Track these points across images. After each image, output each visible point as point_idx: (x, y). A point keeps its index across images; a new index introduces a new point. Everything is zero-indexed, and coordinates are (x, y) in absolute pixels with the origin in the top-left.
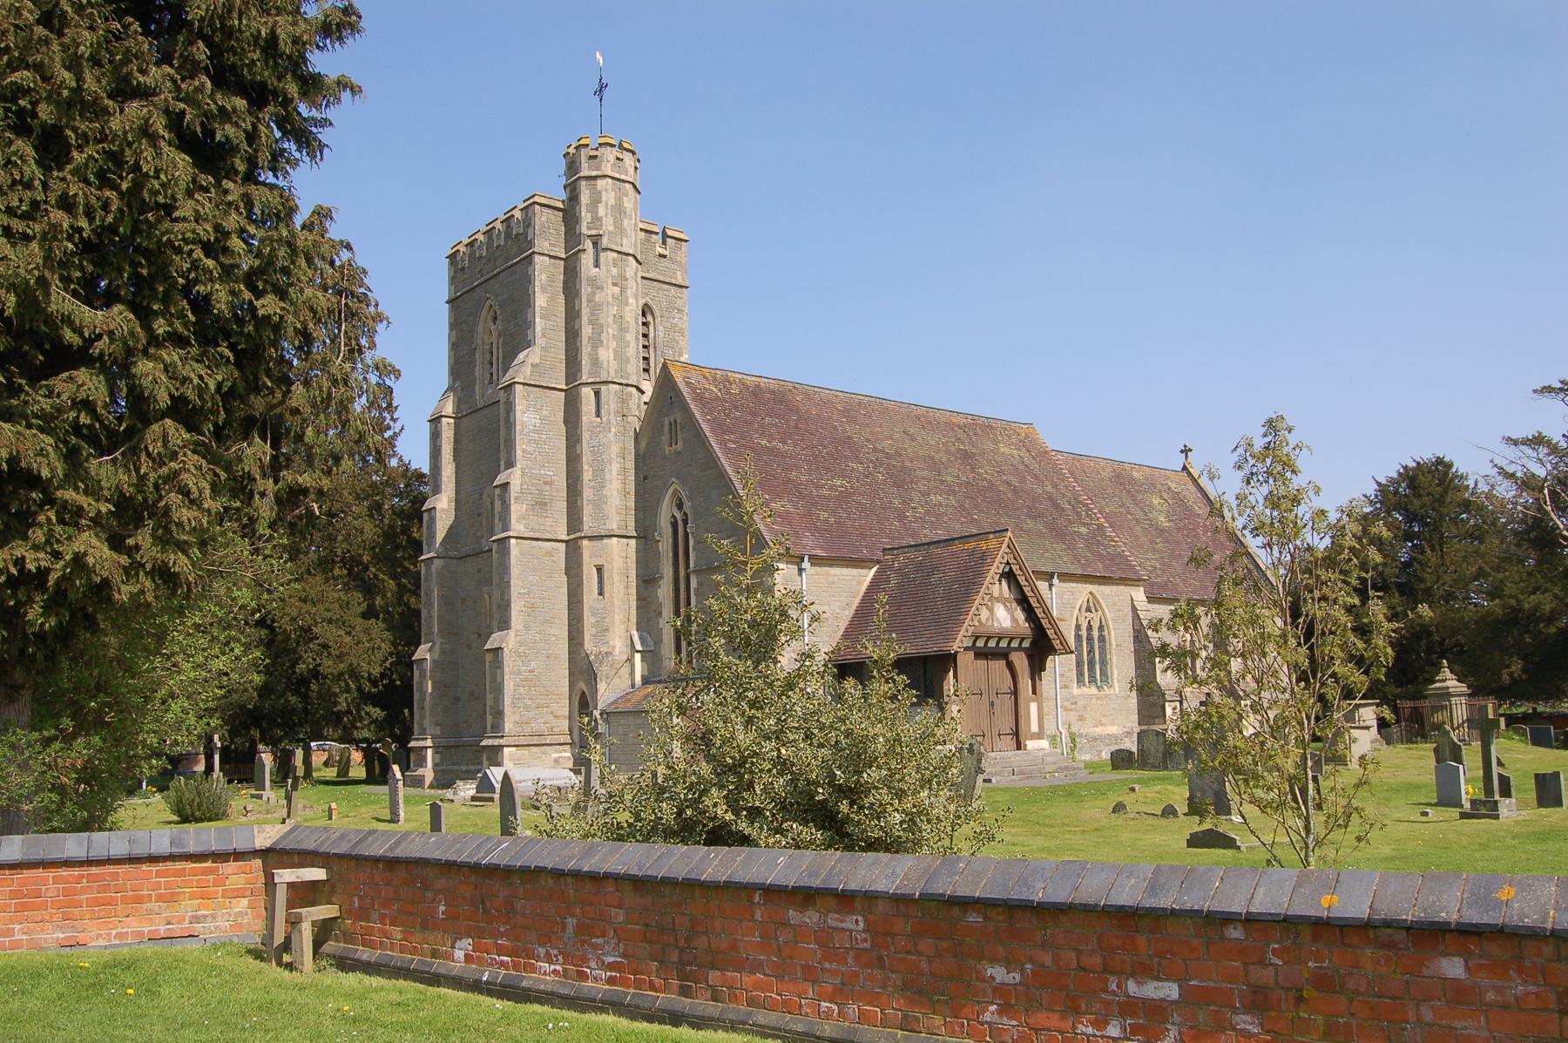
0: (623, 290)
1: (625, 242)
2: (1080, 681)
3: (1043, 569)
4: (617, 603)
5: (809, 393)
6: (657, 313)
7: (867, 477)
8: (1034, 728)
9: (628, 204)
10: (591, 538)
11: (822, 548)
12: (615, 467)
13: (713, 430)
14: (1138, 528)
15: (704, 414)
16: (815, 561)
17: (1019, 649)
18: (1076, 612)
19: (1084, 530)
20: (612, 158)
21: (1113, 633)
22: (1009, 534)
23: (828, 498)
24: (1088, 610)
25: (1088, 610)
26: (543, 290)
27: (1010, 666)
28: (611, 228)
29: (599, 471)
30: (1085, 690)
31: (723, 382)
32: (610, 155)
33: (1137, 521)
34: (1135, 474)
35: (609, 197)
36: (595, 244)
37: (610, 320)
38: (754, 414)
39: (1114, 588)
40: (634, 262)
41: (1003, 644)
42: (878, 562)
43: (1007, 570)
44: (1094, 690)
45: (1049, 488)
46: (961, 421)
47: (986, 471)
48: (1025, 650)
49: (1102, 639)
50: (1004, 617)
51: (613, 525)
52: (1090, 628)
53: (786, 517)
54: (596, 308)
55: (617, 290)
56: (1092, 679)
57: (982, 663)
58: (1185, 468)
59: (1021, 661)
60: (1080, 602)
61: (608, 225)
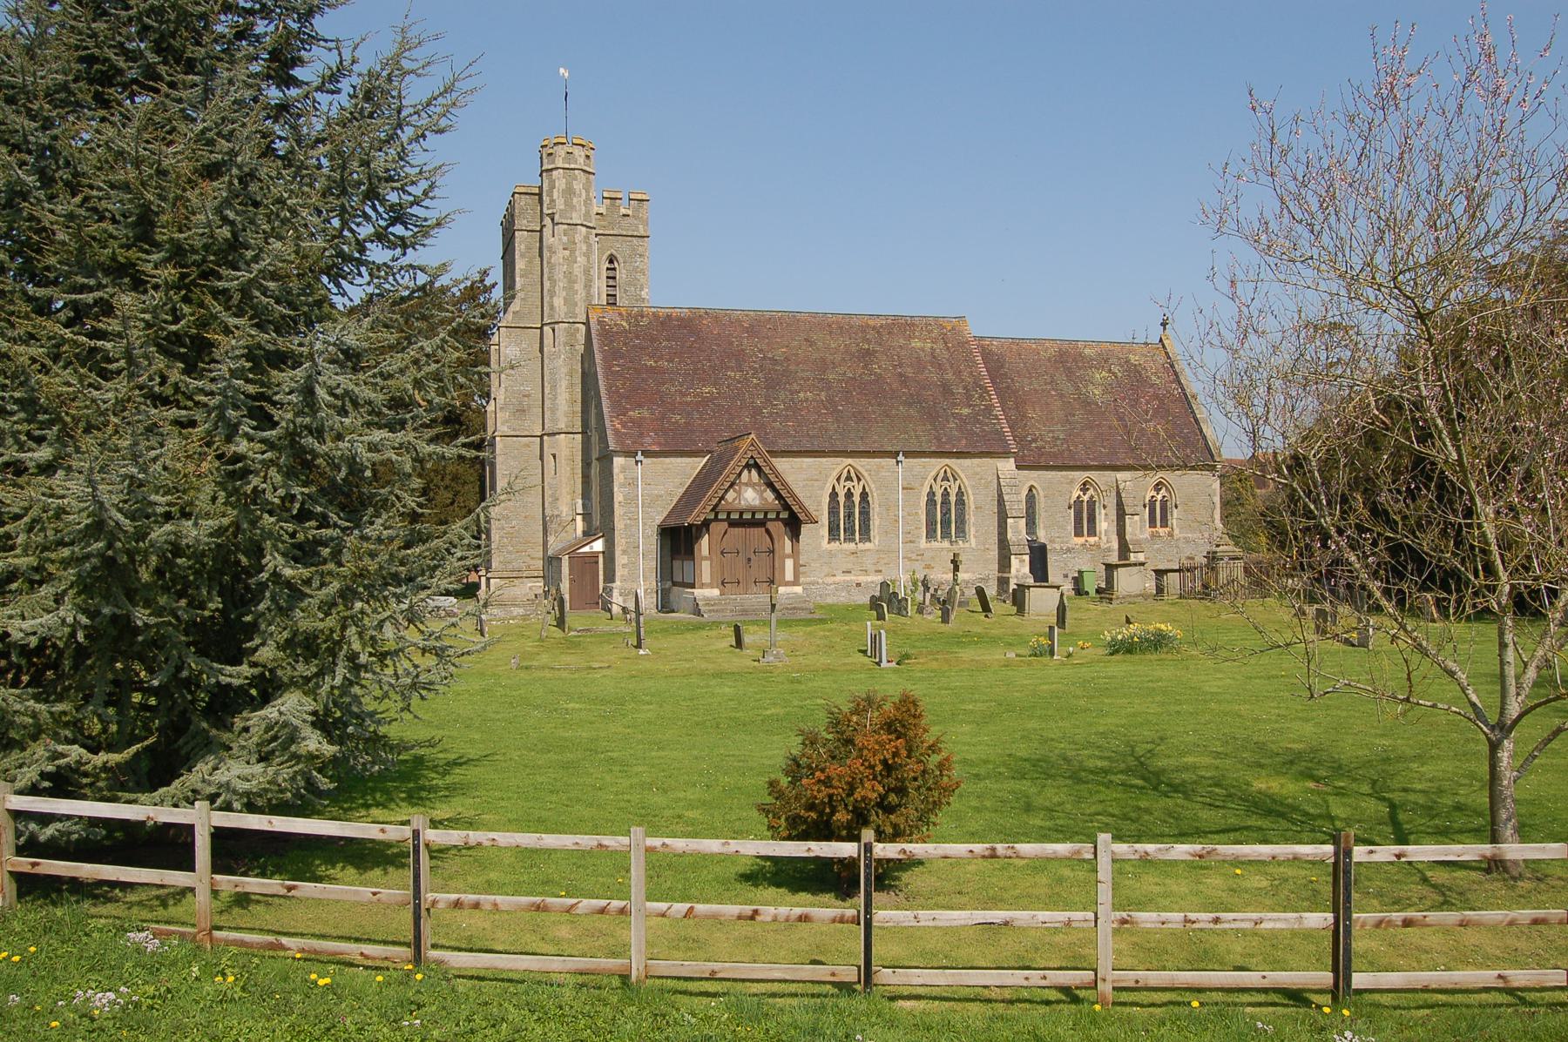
0: (573, 252)
1: (574, 215)
2: (931, 534)
3: (890, 449)
4: (564, 480)
5: (716, 317)
6: (621, 260)
7: (739, 382)
8: (789, 576)
9: (578, 186)
10: (549, 435)
11: (660, 444)
12: (564, 383)
13: (604, 359)
14: (1059, 403)
15: (602, 345)
16: (646, 454)
17: (777, 518)
18: (930, 480)
19: (966, 411)
20: (563, 154)
21: (972, 498)
22: (752, 436)
23: (688, 404)
24: (945, 478)
25: (945, 478)
26: (522, 256)
27: (768, 531)
28: (562, 207)
29: (554, 387)
30: (934, 544)
31: (636, 317)
32: (561, 151)
33: (1062, 396)
34: (1087, 351)
35: (561, 184)
36: (553, 220)
37: (562, 274)
38: (653, 340)
39: (976, 461)
40: (584, 229)
41: (759, 516)
42: (710, 452)
43: (752, 462)
44: (946, 544)
45: (950, 376)
46: (879, 322)
47: (882, 365)
48: (783, 520)
49: (961, 502)
50: (751, 496)
51: (562, 426)
52: (946, 494)
53: (638, 423)
54: (552, 267)
55: (567, 253)
56: (946, 534)
57: (737, 531)
58: (1161, 340)
59: (777, 528)
60: (933, 473)
61: (560, 204)
